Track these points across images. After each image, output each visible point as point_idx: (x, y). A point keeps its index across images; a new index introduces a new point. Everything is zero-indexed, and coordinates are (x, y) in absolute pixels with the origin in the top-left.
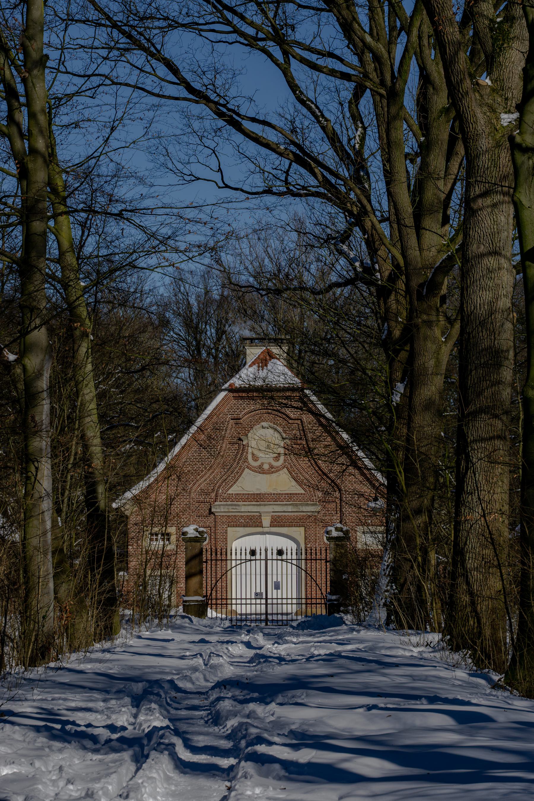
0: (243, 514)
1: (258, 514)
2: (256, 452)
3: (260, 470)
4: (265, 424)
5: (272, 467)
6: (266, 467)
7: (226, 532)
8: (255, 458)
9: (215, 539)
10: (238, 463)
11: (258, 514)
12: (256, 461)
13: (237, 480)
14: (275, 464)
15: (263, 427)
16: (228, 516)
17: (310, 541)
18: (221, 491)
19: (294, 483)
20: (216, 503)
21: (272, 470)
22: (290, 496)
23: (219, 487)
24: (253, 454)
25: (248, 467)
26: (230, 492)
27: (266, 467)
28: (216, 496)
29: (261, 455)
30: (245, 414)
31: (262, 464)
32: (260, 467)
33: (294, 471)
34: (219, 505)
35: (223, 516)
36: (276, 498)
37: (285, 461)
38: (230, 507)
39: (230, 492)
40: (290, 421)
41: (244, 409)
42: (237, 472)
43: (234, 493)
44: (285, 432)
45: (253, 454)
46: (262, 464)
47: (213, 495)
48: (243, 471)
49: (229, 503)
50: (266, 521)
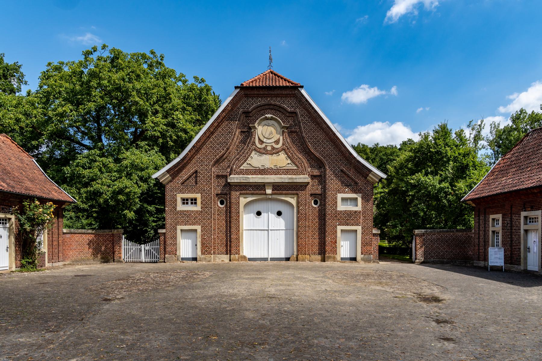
2: (262, 138)
3: (263, 152)
5: (273, 148)
6: (269, 148)
8: (261, 142)
9: (230, 203)
10: (248, 146)
15: (267, 119)
16: (241, 186)
17: (301, 205)
18: (235, 166)
19: (289, 161)
20: (231, 176)
21: (274, 152)
22: (287, 172)
23: (233, 164)
24: (259, 139)
25: (255, 150)
26: (242, 168)
27: (269, 148)
28: (231, 170)
29: (265, 140)
30: (254, 109)
31: (266, 146)
32: (265, 148)
33: (290, 152)
34: (234, 178)
35: (236, 186)
36: (277, 171)
37: (283, 144)
38: (242, 179)
39: (242, 168)
40: (288, 114)
41: (252, 104)
42: (247, 153)
43: (245, 168)
44: (283, 122)
45: (259, 139)
46: (266, 146)
47: (229, 170)
48: (251, 152)
49: (241, 176)
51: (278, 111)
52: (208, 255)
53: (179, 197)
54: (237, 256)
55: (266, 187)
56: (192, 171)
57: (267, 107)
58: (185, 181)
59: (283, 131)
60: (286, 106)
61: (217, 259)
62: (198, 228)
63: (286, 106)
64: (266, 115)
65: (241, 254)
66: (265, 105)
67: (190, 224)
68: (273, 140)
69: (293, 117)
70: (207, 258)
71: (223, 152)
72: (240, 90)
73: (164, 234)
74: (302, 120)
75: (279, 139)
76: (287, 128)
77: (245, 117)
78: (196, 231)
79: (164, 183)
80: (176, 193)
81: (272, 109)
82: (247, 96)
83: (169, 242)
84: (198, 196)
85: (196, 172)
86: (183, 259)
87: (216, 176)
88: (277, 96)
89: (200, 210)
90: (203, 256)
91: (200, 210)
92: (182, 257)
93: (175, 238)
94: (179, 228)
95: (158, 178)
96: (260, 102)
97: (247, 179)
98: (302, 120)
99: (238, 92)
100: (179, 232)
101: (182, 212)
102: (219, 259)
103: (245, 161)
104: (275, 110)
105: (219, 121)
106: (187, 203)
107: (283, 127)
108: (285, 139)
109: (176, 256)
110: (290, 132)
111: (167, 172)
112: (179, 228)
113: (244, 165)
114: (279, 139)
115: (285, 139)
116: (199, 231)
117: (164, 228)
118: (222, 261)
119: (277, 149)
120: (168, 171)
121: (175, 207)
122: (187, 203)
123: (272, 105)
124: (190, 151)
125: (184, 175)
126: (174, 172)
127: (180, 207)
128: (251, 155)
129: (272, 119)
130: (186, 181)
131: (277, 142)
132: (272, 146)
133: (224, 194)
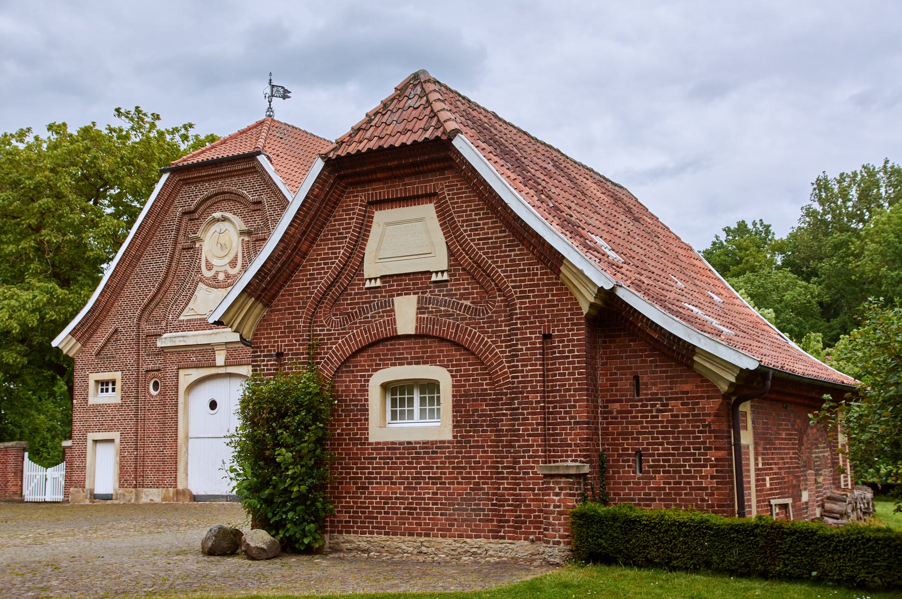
0: (194, 349)
1: (211, 347)
2: (209, 260)
4: (217, 215)
5: (228, 276)
6: (221, 277)
7: (177, 377)
8: (210, 267)
11: (211, 347)
12: (210, 270)
13: (189, 300)
14: (232, 272)
16: (179, 353)
20: (165, 335)
24: (207, 261)
25: (201, 280)
26: (181, 318)
27: (221, 277)
29: (215, 262)
31: (217, 273)
32: (215, 278)
39: (181, 318)
40: (252, 207)
43: (186, 318)
45: (207, 261)
46: (217, 273)
47: (164, 324)
50: (220, 358)
51: (239, 202)
52: (128, 489)
53: (93, 377)
54: (171, 490)
55: (216, 352)
56: (111, 330)
57: (220, 197)
58: (101, 350)
59: (243, 240)
60: (245, 192)
61: (143, 496)
62: (116, 435)
63: (245, 192)
64: (214, 215)
65: (180, 487)
66: (216, 195)
67: (105, 430)
68: (227, 260)
69: (260, 210)
70: (126, 494)
71: (154, 290)
72: (171, 174)
73: (70, 447)
74: (271, 215)
75: (236, 258)
76: (249, 233)
77: (190, 220)
78: (112, 441)
79: (71, 355)
80: (88, 373)
81: (229, 200)
82: (187, 182)
83: (77, 463)
84: (117, 376)
85: (116, 331)
86: (94, 497)
87: (147, 336)
88: (230, 175)
89: (120, 402)
90: (121, 491)
91: (120, 402)
92: (96, 493)
93: (83, 455)
94: (91, 436)
95: (60, 347)
96: (208, 189)
97: (185, 339)
98: (271, 215)
99: (169, 178)
100: (90, 443)
101: (96, 407)
102: (147, 496)
103: (187, 304)
104: (233, 200)
105: (143, 234)
106: (107, 391)
107: (242, 233)
108: (245, 255)
109: (85, 490)
110: (257, 240)
111: (70, 336)
112: (91, 436)
113: (184, 313)
114: (236, 258)
115: (245, 255)
116: (117, 441)
117: (70, 438)
118: (151, 500)
119: (234, 276)
120: (73, 333)
121: (86, 400)
122: (107, 391)
123: (228, 193)
124: (101, 295)
125: (100, 339)
126: (84, 333)
127: (97, 398)
128: (195, 293)
129: (224, 219)
130: (102, 348)
131: (233, 264)
132: (226, 272)
133: (156, 371)
